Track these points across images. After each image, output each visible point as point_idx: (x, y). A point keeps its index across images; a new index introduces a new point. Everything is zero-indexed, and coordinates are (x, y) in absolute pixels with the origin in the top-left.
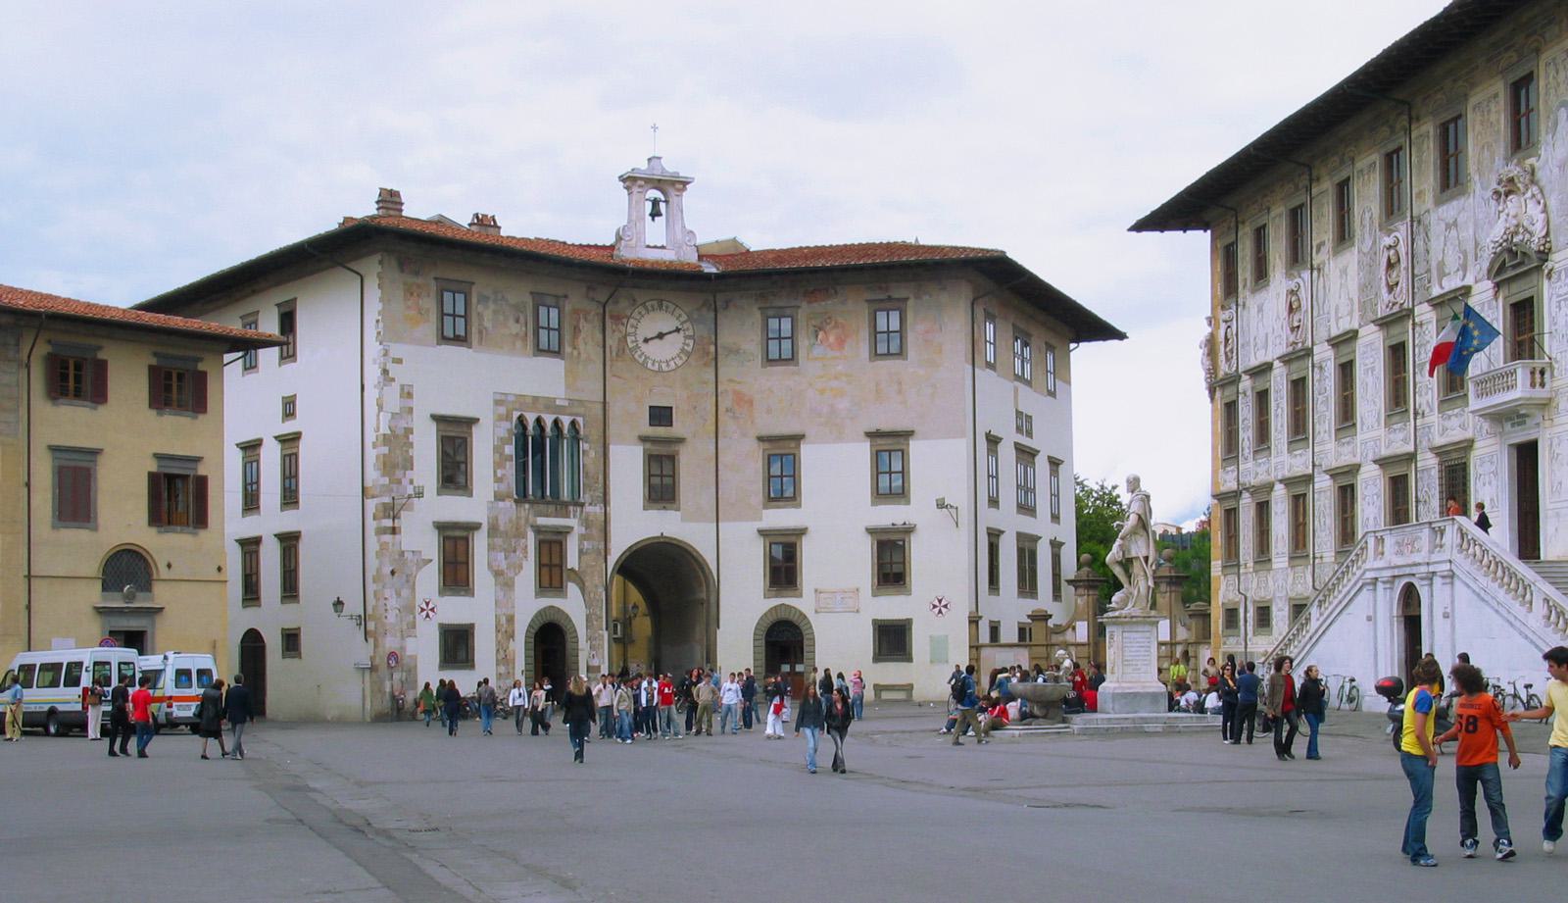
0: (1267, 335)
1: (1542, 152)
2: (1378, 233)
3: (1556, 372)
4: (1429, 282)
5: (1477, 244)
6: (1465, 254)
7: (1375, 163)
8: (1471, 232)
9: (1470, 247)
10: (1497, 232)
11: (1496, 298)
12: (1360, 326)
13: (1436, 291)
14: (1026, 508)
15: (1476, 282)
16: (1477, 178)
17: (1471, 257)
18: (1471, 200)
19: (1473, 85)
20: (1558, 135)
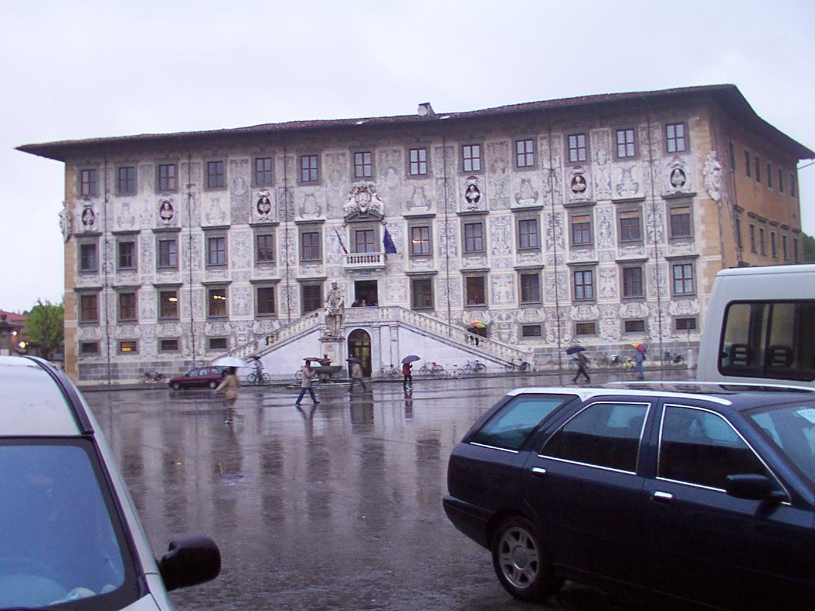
0: (133, 218)
1: (378, 181)
2: (250, 188)
3: (388, 258)
4: (293, 214)
5: (328, 205)
6: (320, 208)
7: (247, 160)
8: (324, 199)
9: (324, 206)
10: (352, 203)
11: (344, 227)
12: (232, 224)
13: (298, 219)
15: (328, 219)
16: (329, 181)
17: (324, 210)
18: (324, 188)
19: (327, 147)
20: (387, 177)
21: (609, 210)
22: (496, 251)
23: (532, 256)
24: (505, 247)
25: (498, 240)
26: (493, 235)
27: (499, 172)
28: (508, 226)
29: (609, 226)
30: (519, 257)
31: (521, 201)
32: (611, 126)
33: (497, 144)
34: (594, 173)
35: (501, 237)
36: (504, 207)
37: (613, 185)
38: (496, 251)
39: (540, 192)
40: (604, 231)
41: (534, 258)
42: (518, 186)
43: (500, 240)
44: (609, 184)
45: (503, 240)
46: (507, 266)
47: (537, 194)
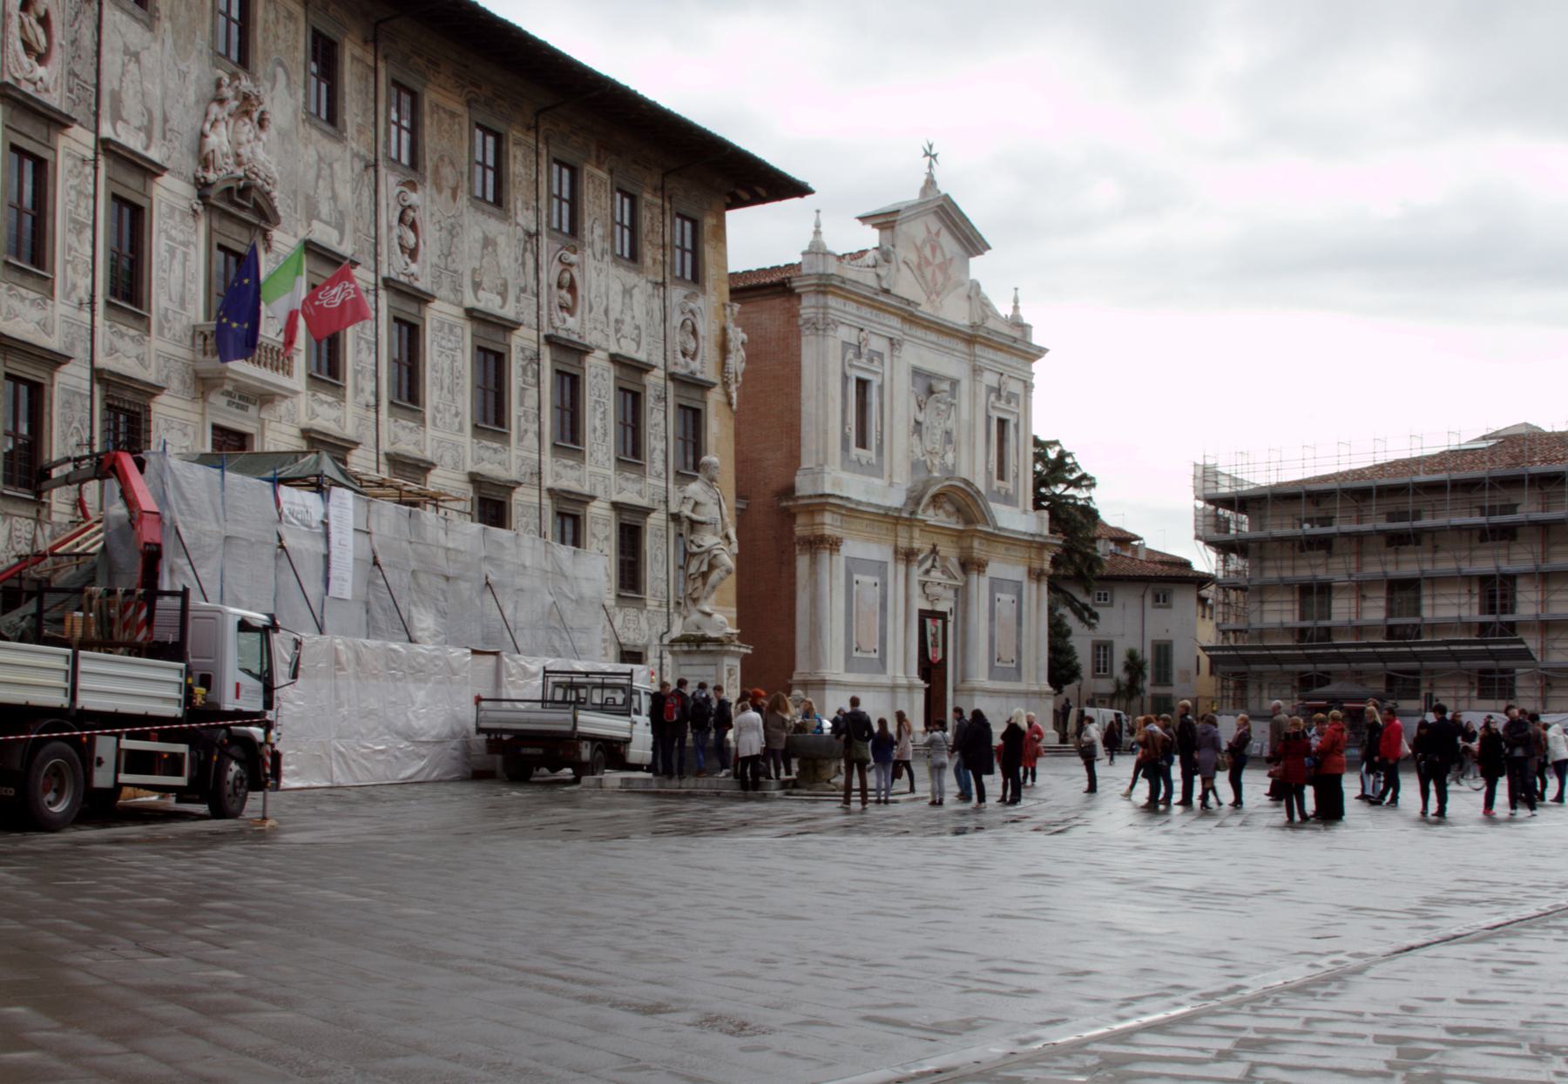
14: (632, 452)
21: (606, 375)
22: (439, 416)
23: (495, 451)
24: (453, 411)
25: (442, 388)
26: (434, 366)
27: (447, 193)
28: (458, 353)
29: (604, 412)
30: (476, 447)
31: (481, 294)
32: (611, 172)
33: (445, 111)
34: (587, 274)
35: (447, 382)
36: (452, 297)
37: (612, 317)
38: (439, 416)
39: (510, 282)
40: (598, 423)
41: (499, 457)
42: (477, 253)
43: (445, 386)
44: (606, 312)
45: (451, 392)
46: (455, 467)
47: (505, 285)
